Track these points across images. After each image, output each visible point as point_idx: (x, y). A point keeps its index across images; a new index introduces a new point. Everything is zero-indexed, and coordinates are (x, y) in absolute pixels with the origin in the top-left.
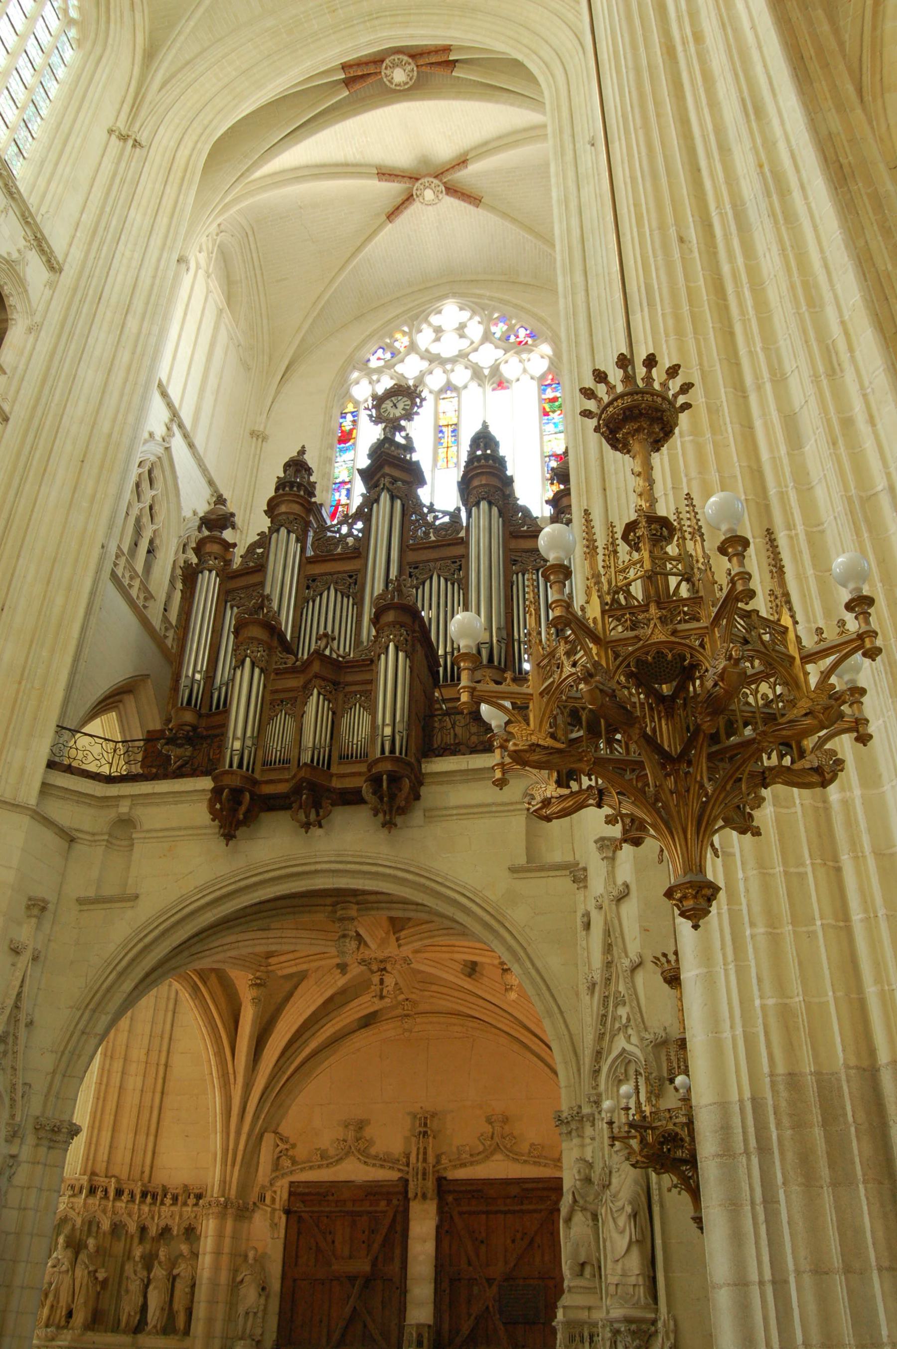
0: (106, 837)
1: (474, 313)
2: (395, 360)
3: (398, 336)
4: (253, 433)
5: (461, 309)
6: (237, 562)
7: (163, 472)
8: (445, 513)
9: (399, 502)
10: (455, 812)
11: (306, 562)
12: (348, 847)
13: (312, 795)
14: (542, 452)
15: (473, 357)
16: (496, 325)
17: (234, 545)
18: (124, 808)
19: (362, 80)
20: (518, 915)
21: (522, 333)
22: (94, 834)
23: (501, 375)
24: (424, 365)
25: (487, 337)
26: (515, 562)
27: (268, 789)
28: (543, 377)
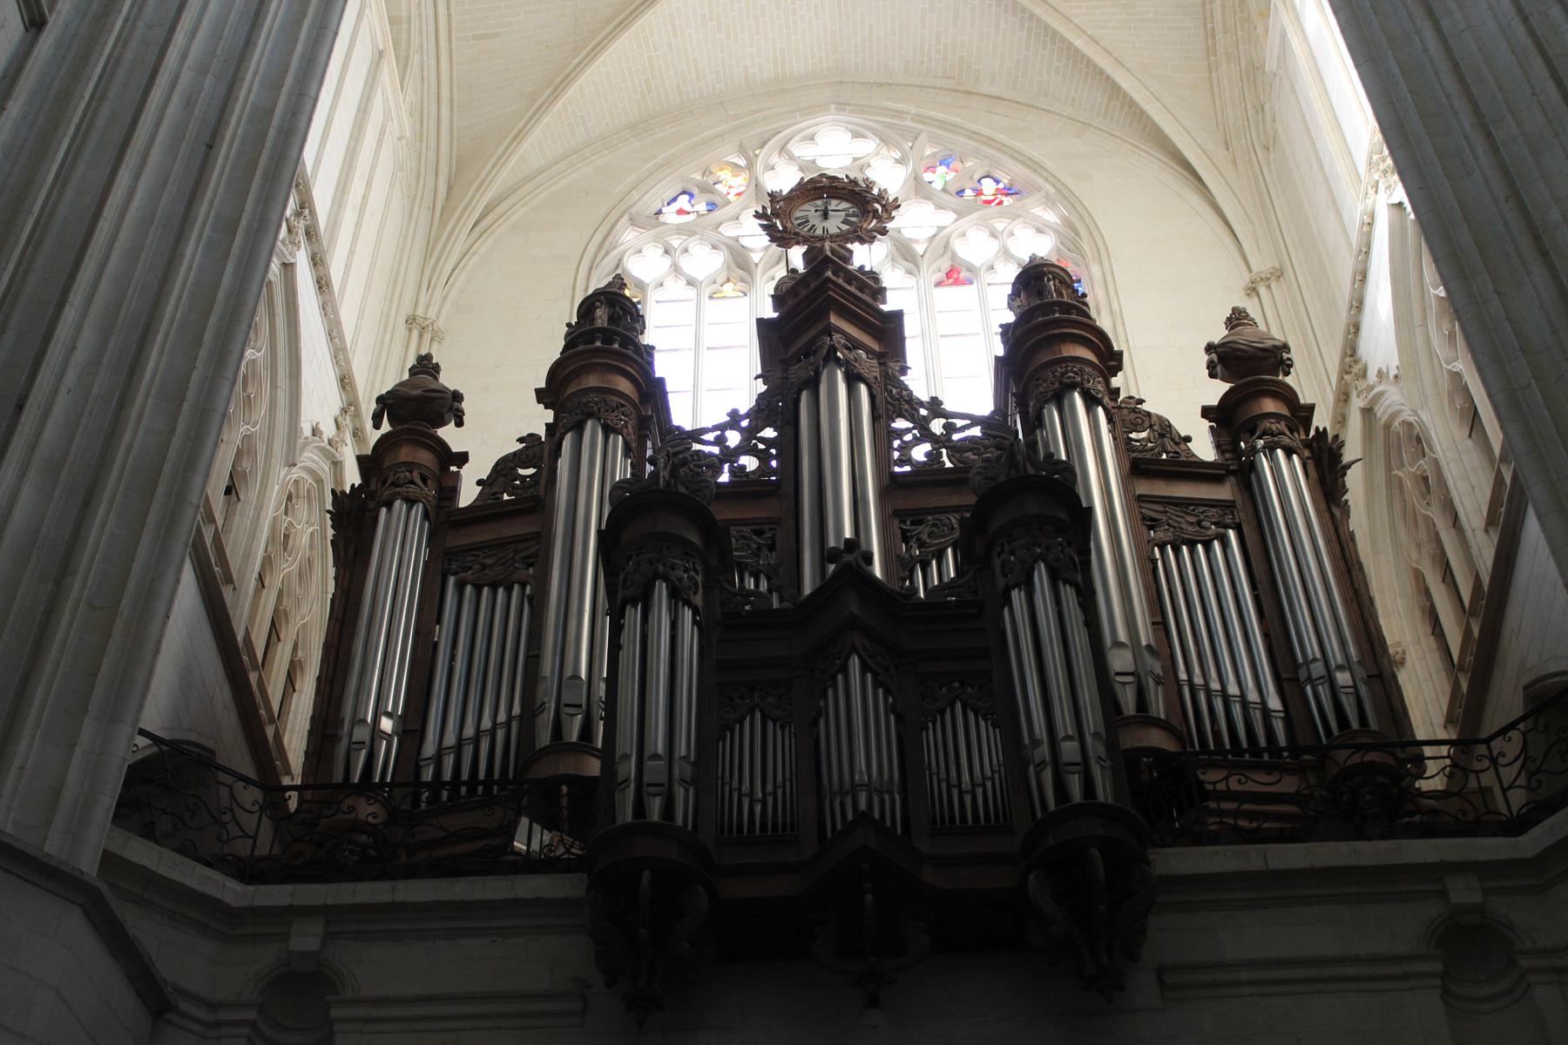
0: (252, 1015)
1: (884, 140)
2: (718, 215)
4: (411, 321)
5: (856, 135)
6: (468, 494)
7: (272, 316)
8: (975, 421)
9: (863, 388)
10: (1244, 975)
16: (931, 169)
17: (463, 458)
18: (306, 939)
22: (213, 1007)
23: (954, 256)
26: (1152, 523)
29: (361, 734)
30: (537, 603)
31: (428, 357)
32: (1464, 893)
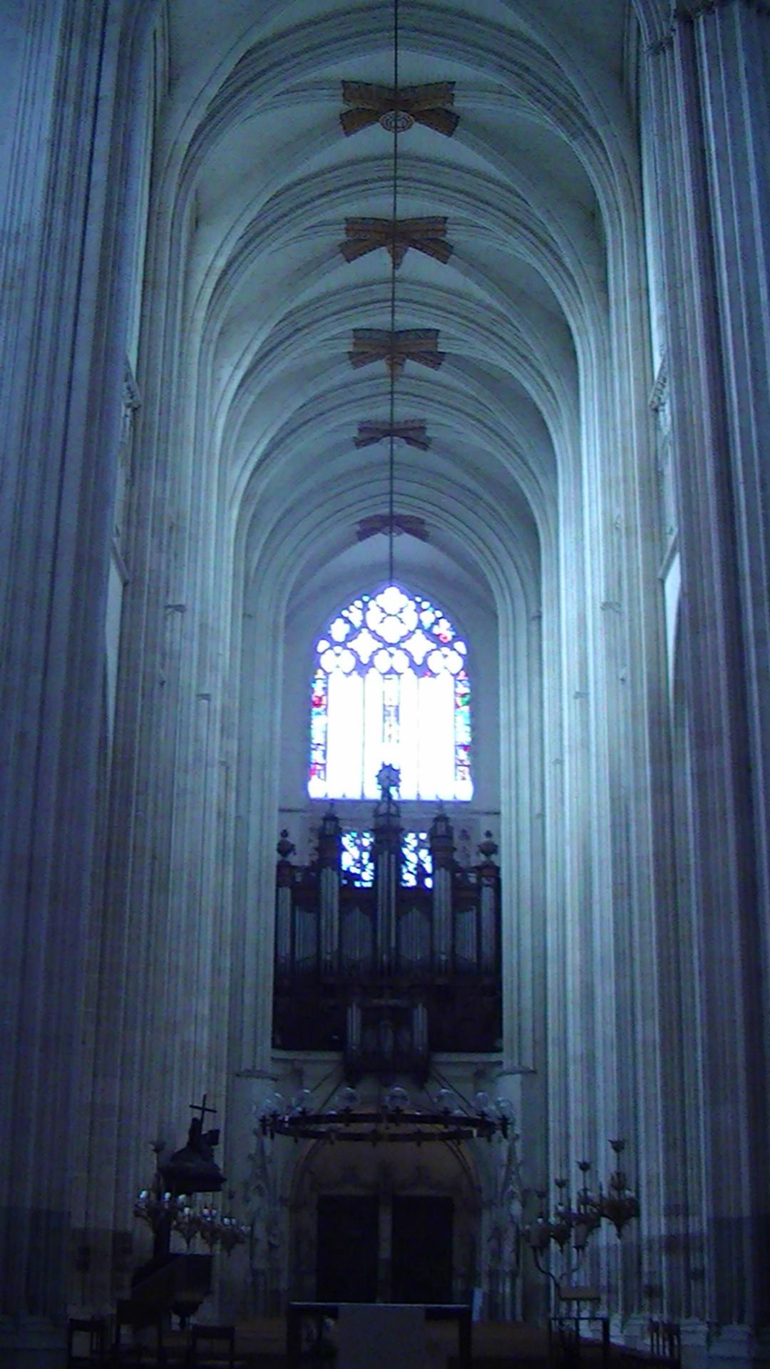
3: (352, 608)
25: (420, 625)
28: (455, 675)
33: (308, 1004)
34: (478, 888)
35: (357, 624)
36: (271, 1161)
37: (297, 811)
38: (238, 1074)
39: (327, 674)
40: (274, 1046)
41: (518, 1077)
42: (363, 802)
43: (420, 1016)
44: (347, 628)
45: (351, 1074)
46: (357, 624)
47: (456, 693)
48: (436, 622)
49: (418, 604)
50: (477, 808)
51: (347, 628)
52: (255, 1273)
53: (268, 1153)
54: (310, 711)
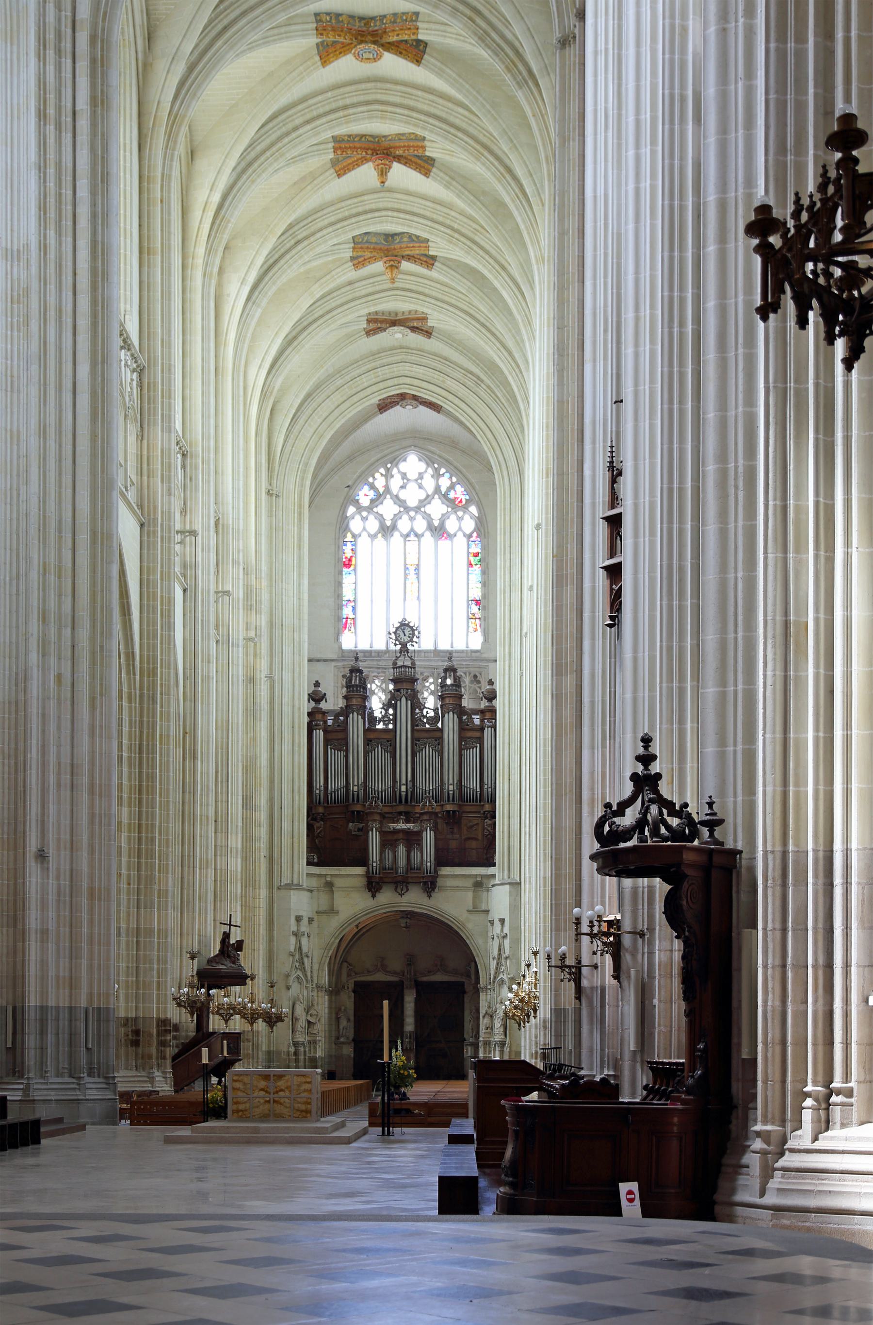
3: (377, 475)
11: (365, 731)
12: (413, 899)
13: (401, 882)
14: (468, 597)
15: (428, 509)
18: (328, 879)
19: (384, 406)
20: (470, 926)
21: (459, 488)
24: (396, 509)
25: (437, 490)
27: (386, 880)
28: (470, 536)
29: (318, 792)
30: (347, 757)
31: (317, 681)
32: (479, 879)
33: (335, 831)
34: (482, 729)
35: (381, 490)
36: (307, 956)
37: (333, 660)
38: (277, 888)
39: (354, 536)
40: (309, 863)
41: (507, 886)
42: (387, 651)
43: (428, 838)
44: (372, 494)
45: (373, 886)
46: (381, 490)
47: (469, 553)
48: (452, 487)
49: (437, 470)
50: (485, 656)
51: (372, 494)
52: (296, 1044)
53: (305, 949)
54: (340, 573)
